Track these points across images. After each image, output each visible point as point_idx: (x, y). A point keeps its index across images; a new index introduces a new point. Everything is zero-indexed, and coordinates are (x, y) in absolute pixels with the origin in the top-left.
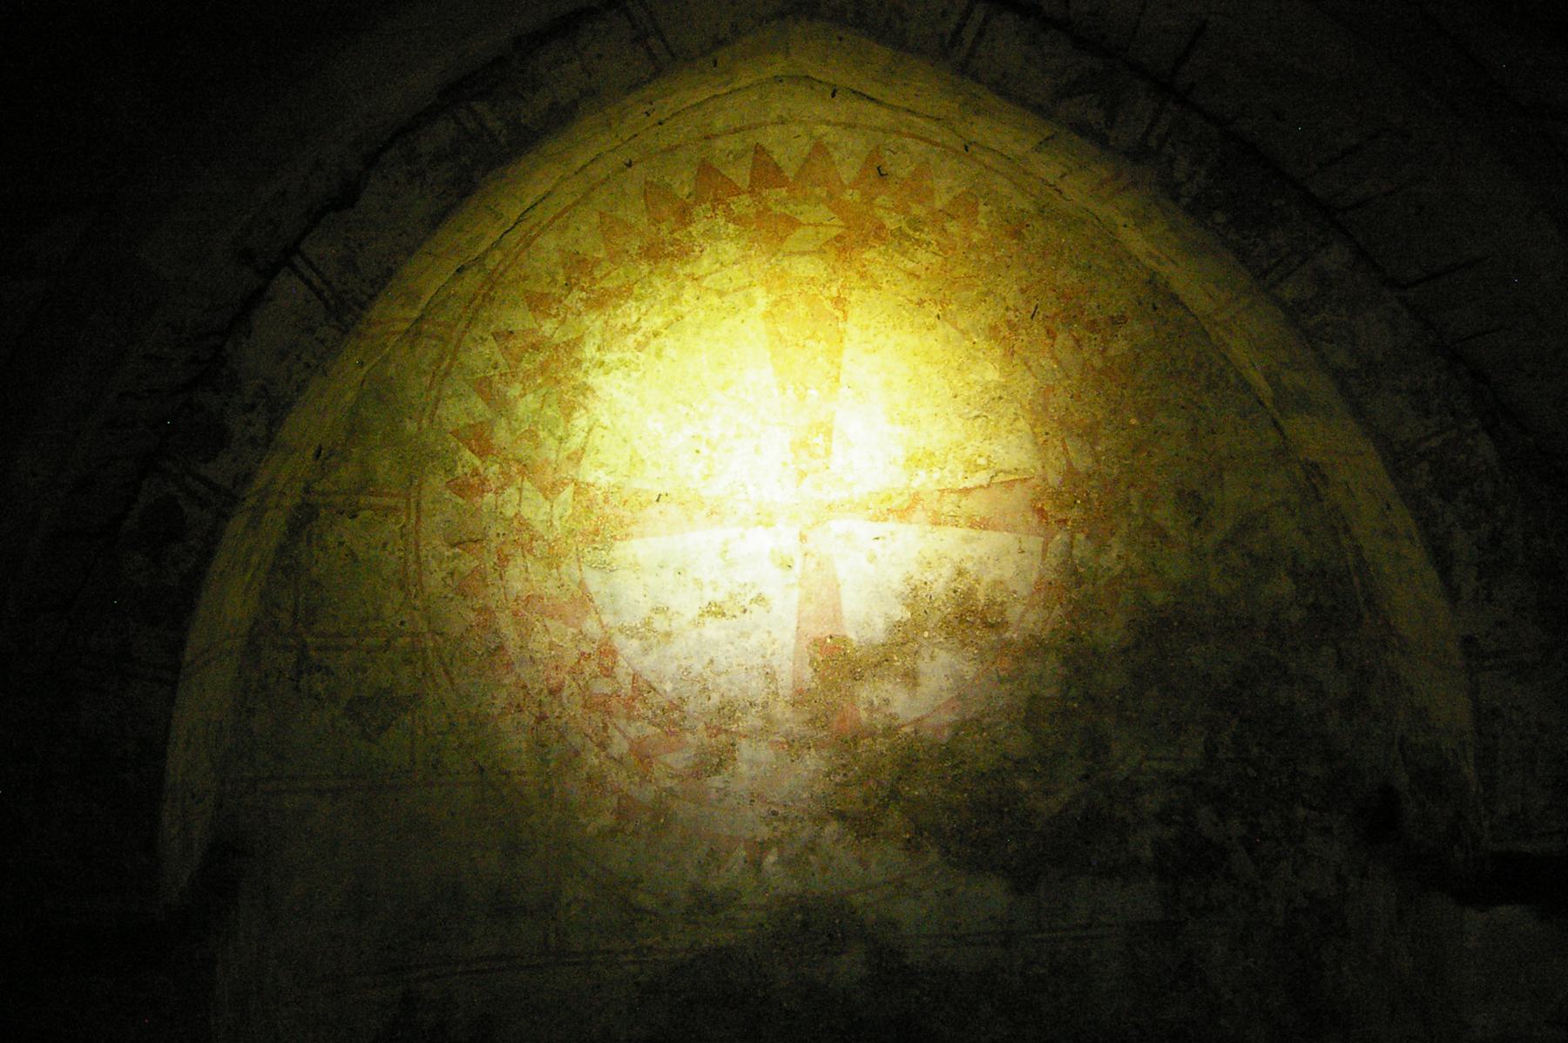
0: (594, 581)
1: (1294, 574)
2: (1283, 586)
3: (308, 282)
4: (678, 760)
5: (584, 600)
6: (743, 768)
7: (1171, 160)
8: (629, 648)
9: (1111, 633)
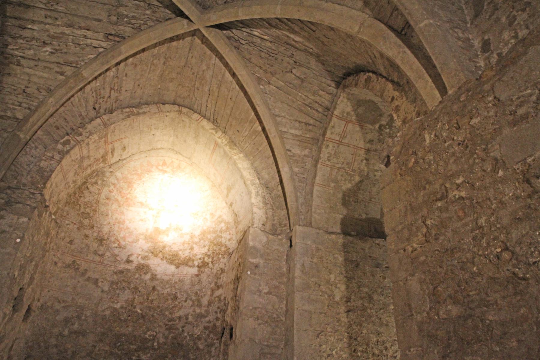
0: (125, 211)
1: (225, 223)
2: (223, 225)
4: (130, 240)
5: (122, 213)
6: (139, 243)
8: (127, 222)
9: (197, 233)
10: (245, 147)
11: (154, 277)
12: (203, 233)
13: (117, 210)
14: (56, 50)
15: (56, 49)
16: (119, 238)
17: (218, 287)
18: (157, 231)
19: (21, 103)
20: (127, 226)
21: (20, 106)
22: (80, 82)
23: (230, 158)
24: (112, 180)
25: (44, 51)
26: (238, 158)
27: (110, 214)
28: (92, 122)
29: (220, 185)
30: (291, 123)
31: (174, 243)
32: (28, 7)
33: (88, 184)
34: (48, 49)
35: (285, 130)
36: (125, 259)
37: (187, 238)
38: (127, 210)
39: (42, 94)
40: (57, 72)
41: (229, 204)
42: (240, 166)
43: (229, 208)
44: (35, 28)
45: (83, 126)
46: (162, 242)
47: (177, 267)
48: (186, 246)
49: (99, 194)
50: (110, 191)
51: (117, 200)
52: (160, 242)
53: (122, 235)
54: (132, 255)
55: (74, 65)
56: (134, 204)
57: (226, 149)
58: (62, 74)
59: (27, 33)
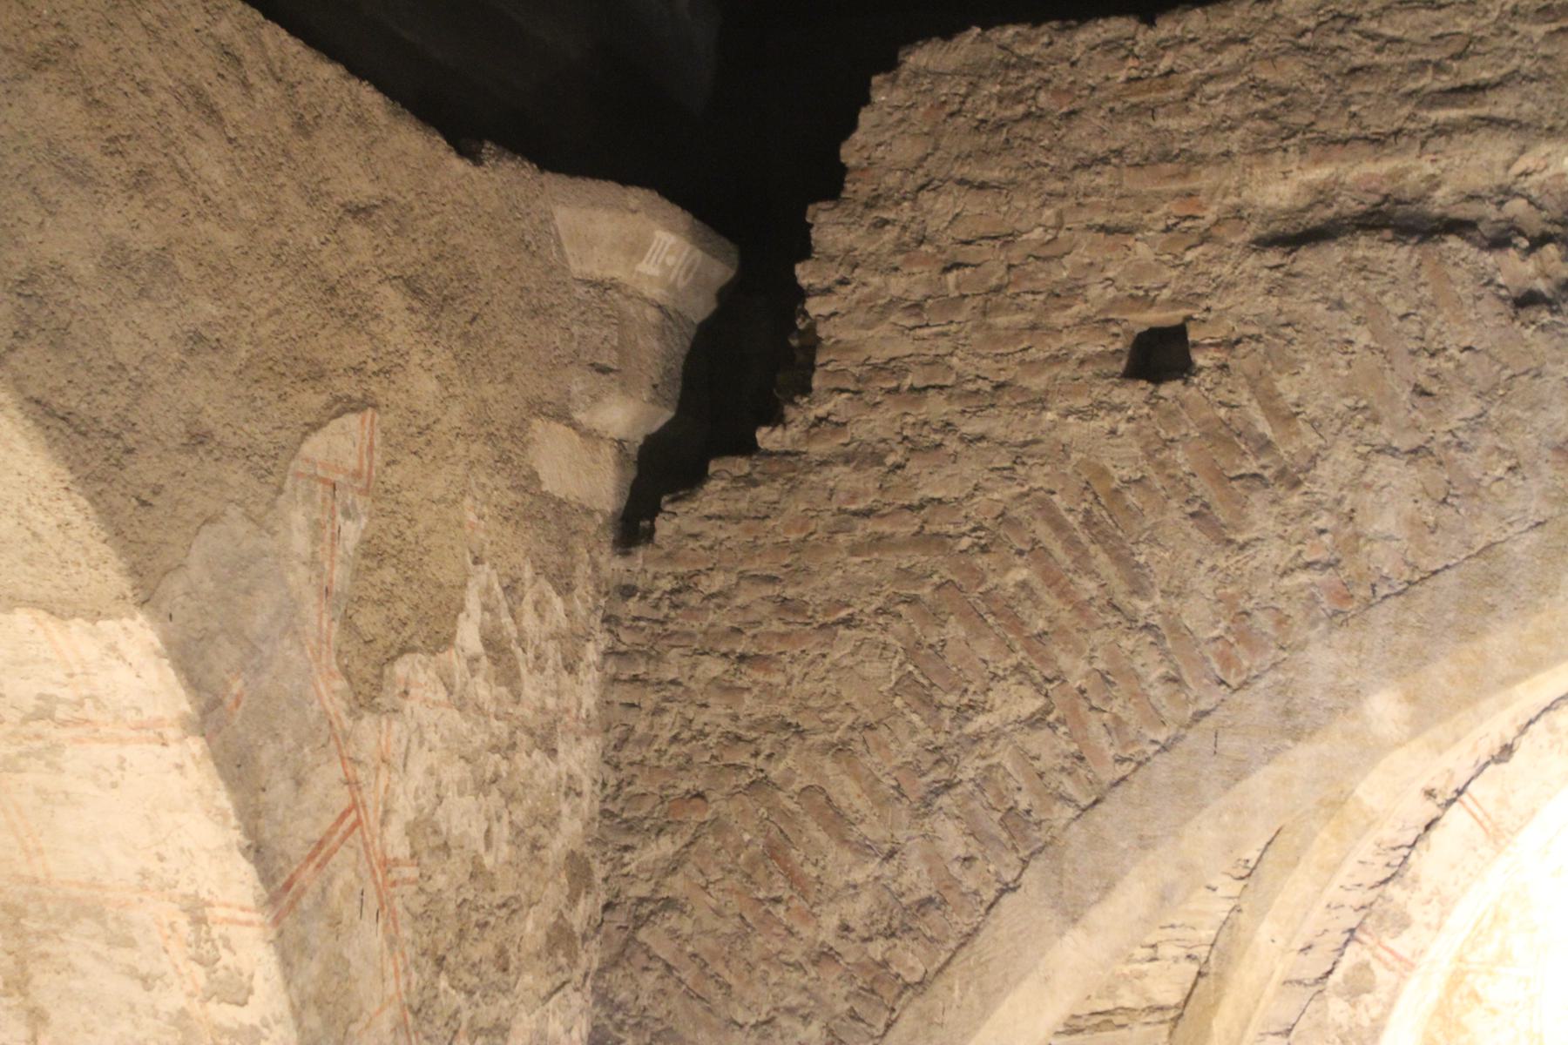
3: (1474, 816)
19: (1154, 946)
21: (1153, 959)
22: (1358, 838)
33: (1470, 977)
39: (1220, 892)
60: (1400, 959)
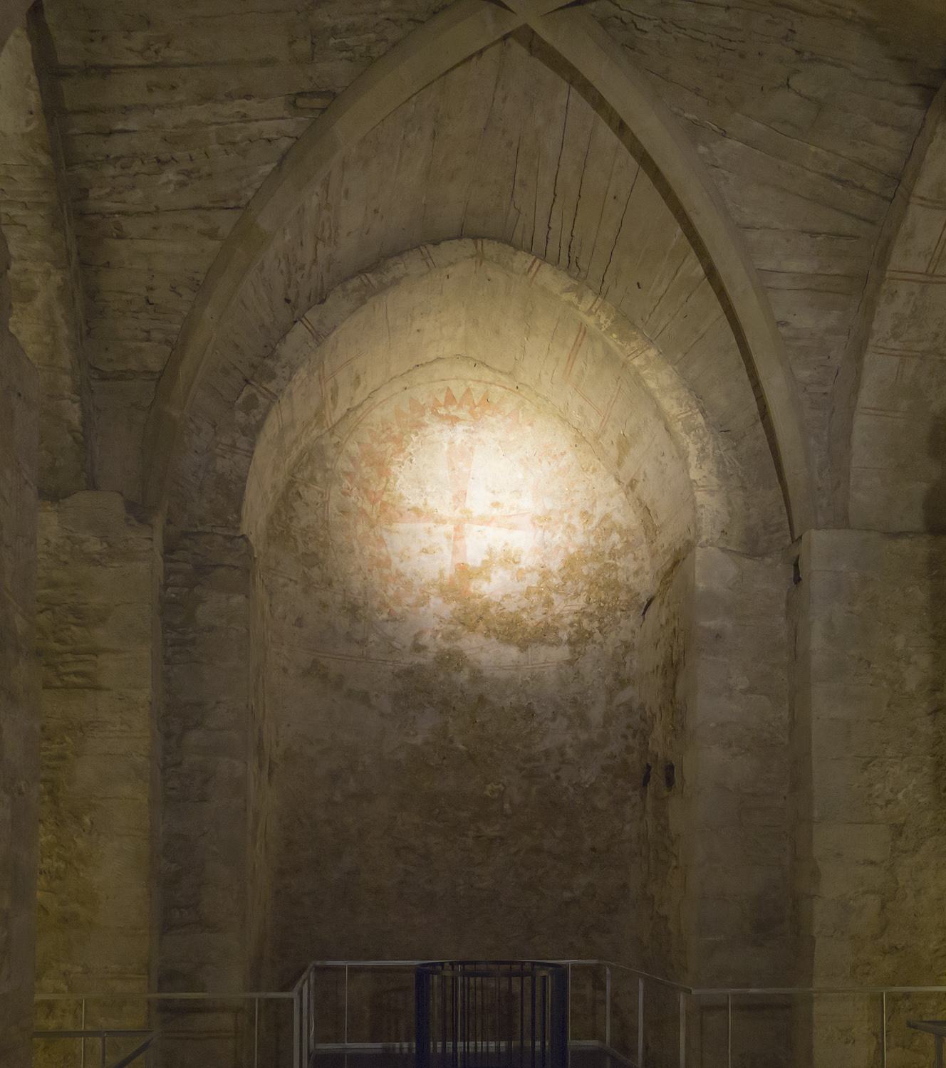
0: (385, 535)
4: (410, 600)
5: (381, 541)
6: (432, 605)
7: (599, 316)
8: (395, 560)
10: (660, 328)
11: (477, 677)
12: (570, 563)
13: (369, 536)
14: (188, 173)
15: (187, 170)
16: (387, 600)
17: (622, 683)
18: (465, 572)
20: (397, 570)
23: (624, 365)
24: (343, 464)
25: (164, 184)
26: (643, 363)
27: (356, 546)
28: (288, 336)
29: (597, 437)
30: (788, 241)
31: (507, 596)
32: (106, 71)
33: (297, 485)
34: (170, 175)
35: (769, 264)
36: (409, 644)
37: (533, 580)
38: (389, 531)
40: (202, 233)
41: (626, 482)
42: (652, 384)
43: (627, 494)
44: (132, 125)
45: (272, 353)
46: (480, 596)
47: (523, 647)
48: (534, 598)
49: (325, 503)
50: (344, 494)
51: (363, 512)
52: (474, 597)
53: (391, 592)
54: (421, 633)
55: (232, 204)
56: (401, 515)
57: (612, 344)
58: (212, 234)
59: (118, 146)
60: (271, 393)
